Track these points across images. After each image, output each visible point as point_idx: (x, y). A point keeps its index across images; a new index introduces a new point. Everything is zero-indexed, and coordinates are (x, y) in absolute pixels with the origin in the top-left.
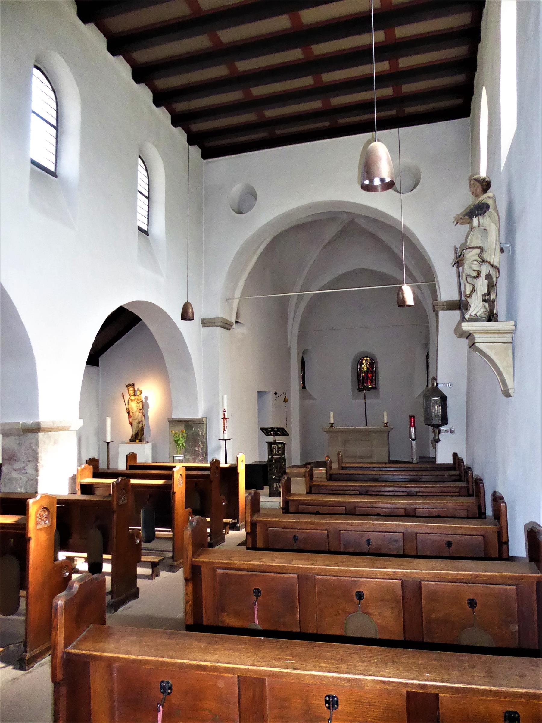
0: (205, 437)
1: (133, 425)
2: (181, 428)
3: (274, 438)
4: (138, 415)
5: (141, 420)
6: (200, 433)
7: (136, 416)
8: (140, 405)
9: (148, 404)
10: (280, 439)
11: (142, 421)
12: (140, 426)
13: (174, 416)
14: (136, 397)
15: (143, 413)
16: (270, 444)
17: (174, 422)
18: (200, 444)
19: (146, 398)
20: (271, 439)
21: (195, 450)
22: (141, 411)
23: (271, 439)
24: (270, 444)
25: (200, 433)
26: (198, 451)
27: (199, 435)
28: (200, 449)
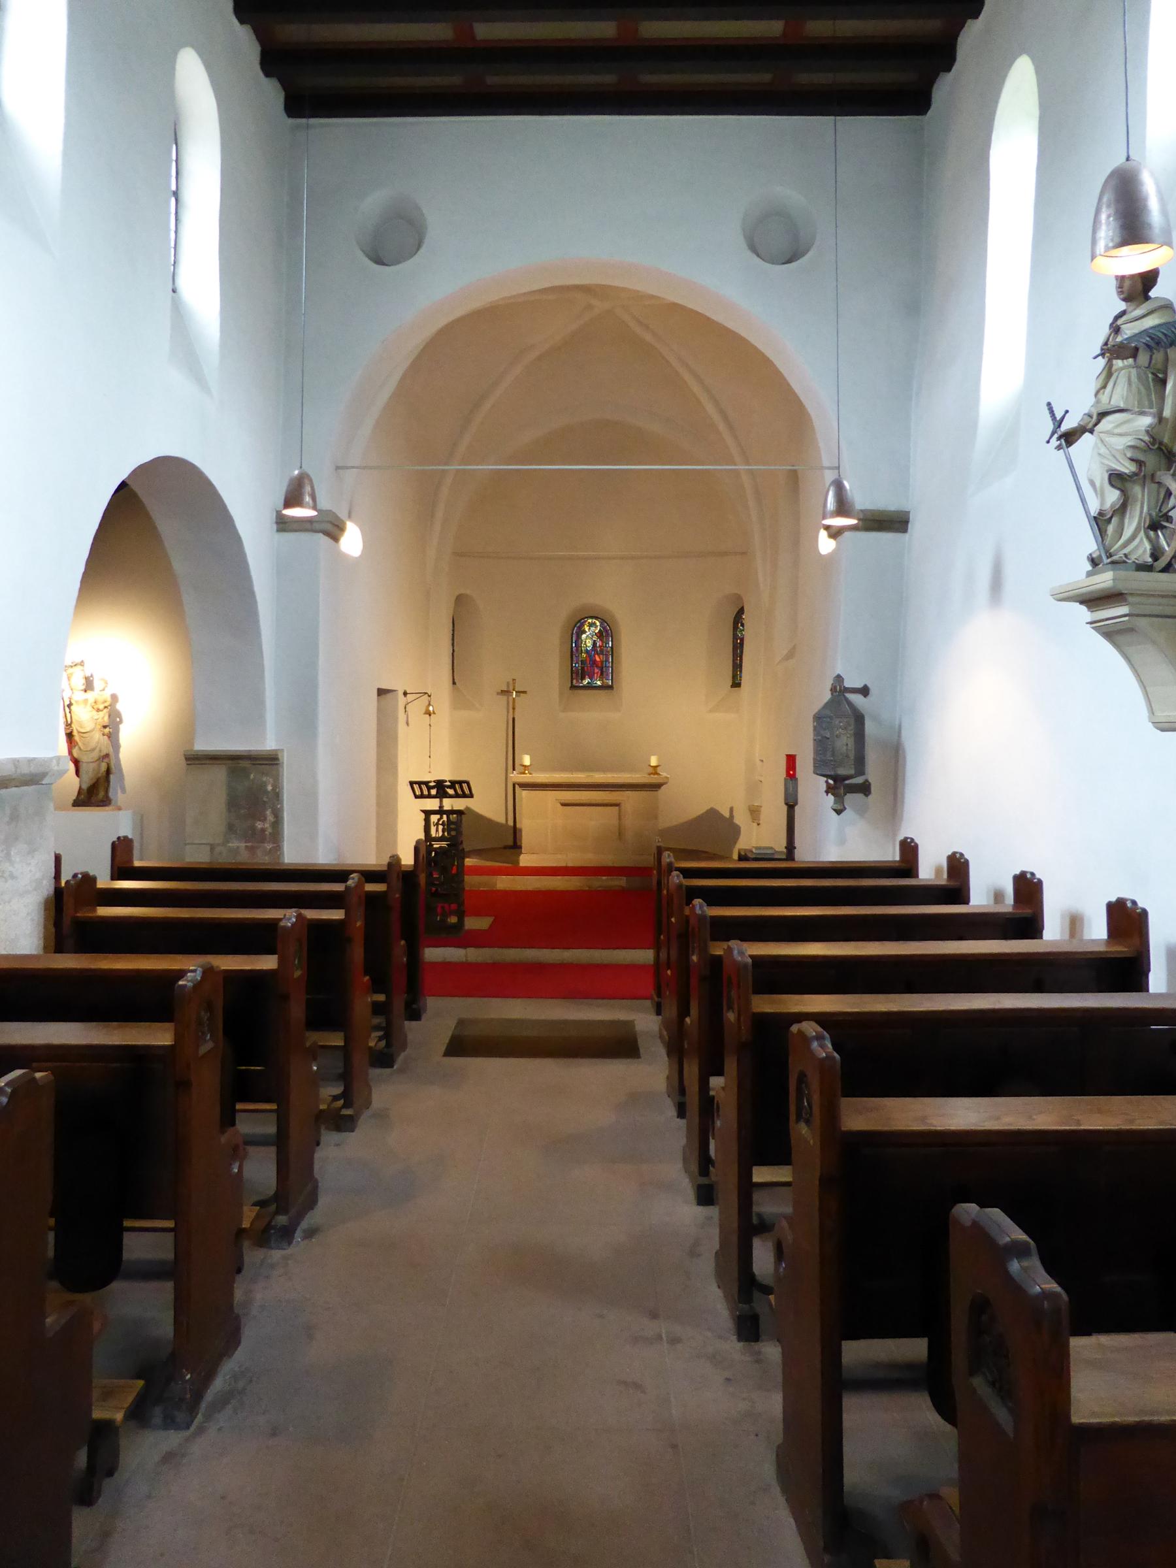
0: (277, 795)
1: (83, 768)
2: (219, 774)
3: (441, 802)
4: (97, 737)
5: (104, 752)
6: (270, 788)
7: (93, 744)
8: (103, 717)
9: (119, 715)
11: (107, 756)
12: (104, 767)
13: (202, 745)
14: (91, 696)
15: (109, 736)
16: (428, 813)
17: (197, 760)
18: (268, 812)
19: (114, 698)
20: (433, 804)
21: (253, 828)
22: (107, 730)
24: (428, 813)
25: (270, 788)
26: (263, 830)
27: (266, 792)
28: (267, 825)
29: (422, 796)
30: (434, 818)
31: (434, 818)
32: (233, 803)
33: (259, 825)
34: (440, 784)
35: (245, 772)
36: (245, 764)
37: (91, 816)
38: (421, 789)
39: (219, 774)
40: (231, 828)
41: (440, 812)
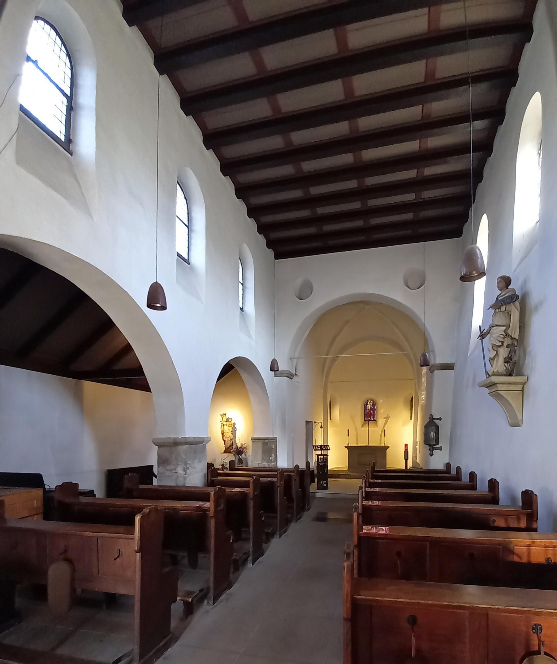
2: (260, 443)
10: (324, 452)
16: (318, 455)
20: (319, 452)
23: (319, 452)
29: (316, 450)
30: (320, 457)
31: (320, 457)
32: (264, 452)
33: (271, 458)
34: (321, 446)
35: (267, 444)
36: (267, 441)
37: (226, 455)
38: (316, 448)
39: (260, 443)
40: (263, 459)
41: (321, 455)
